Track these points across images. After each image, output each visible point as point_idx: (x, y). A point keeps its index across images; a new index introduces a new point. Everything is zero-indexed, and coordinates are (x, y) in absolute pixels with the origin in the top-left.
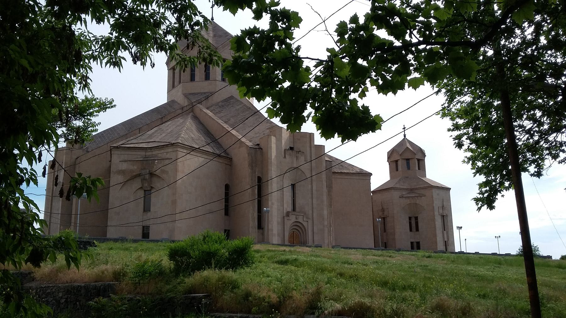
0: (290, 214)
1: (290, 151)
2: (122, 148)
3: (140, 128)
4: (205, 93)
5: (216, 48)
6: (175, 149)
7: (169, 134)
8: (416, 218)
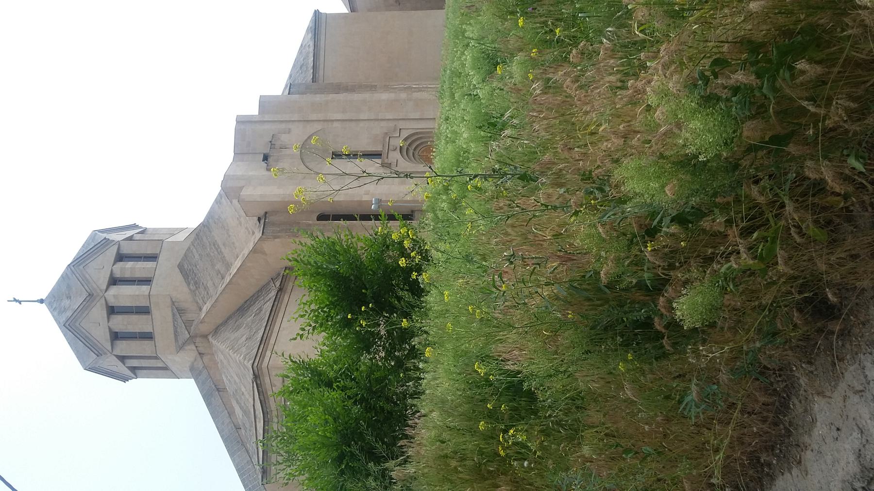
0: (386, 161)
1: (270, 160)
3: (237, 429)
4: (174, 315)
5: (89, 295)
6: (265, 371)
7: (241, 380)
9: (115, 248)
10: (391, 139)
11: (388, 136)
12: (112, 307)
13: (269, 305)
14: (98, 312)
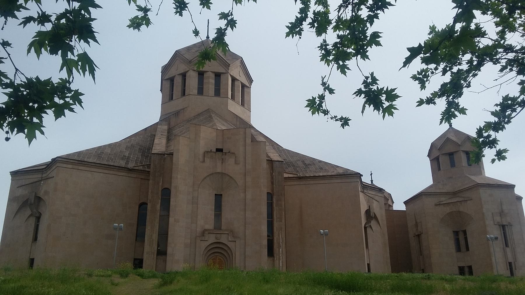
0: (206, 232)
2: (20, 173)
5: (190, 61)
8: (465, 232)
10: (227, 235)
12: (185, 76)
13: (122, 163)
14: (182, 68)
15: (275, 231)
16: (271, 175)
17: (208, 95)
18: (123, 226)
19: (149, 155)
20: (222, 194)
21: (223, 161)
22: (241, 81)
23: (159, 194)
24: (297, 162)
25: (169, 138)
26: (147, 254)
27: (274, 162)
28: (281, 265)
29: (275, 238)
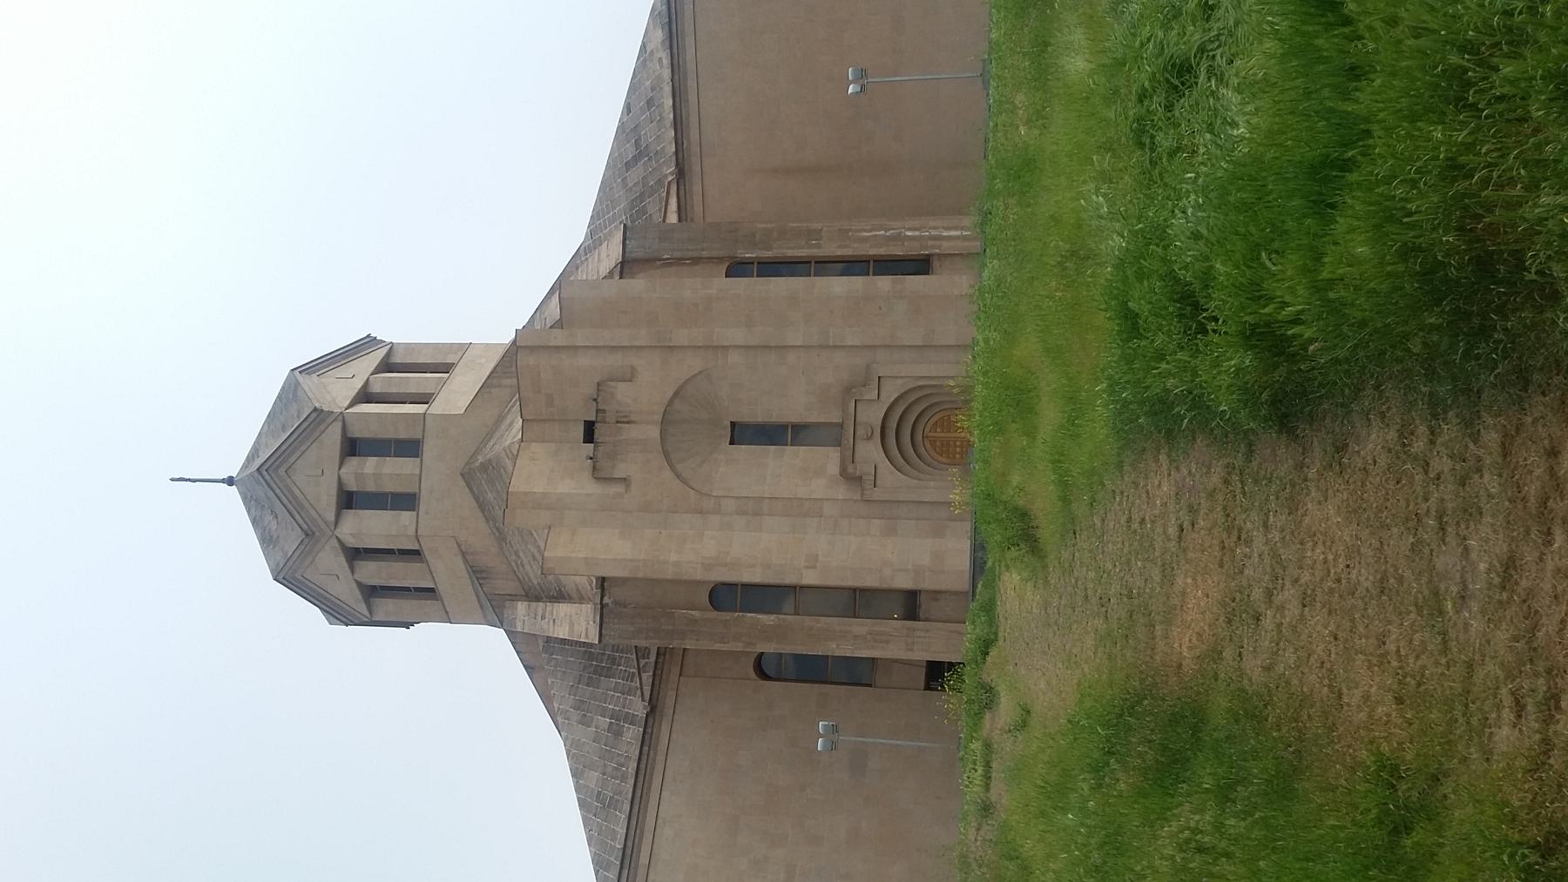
5: (307, 535)
9: (336, 429)
11: (850, 392)
13: (632, 733)
14: (330, 560)
15: (850, 253)
16: (671, 264)
17: (418, 478)
18: (827, 723)
19: (609, 655)
20: (733, 424)
21: (624, 420)
22: (369, 373)
23: (728, 618)
24: (630, 185)
25: (555, 595)
26: (911, 650)
27: (627, 255)
28: (958, 233)
29: (871, 253)
